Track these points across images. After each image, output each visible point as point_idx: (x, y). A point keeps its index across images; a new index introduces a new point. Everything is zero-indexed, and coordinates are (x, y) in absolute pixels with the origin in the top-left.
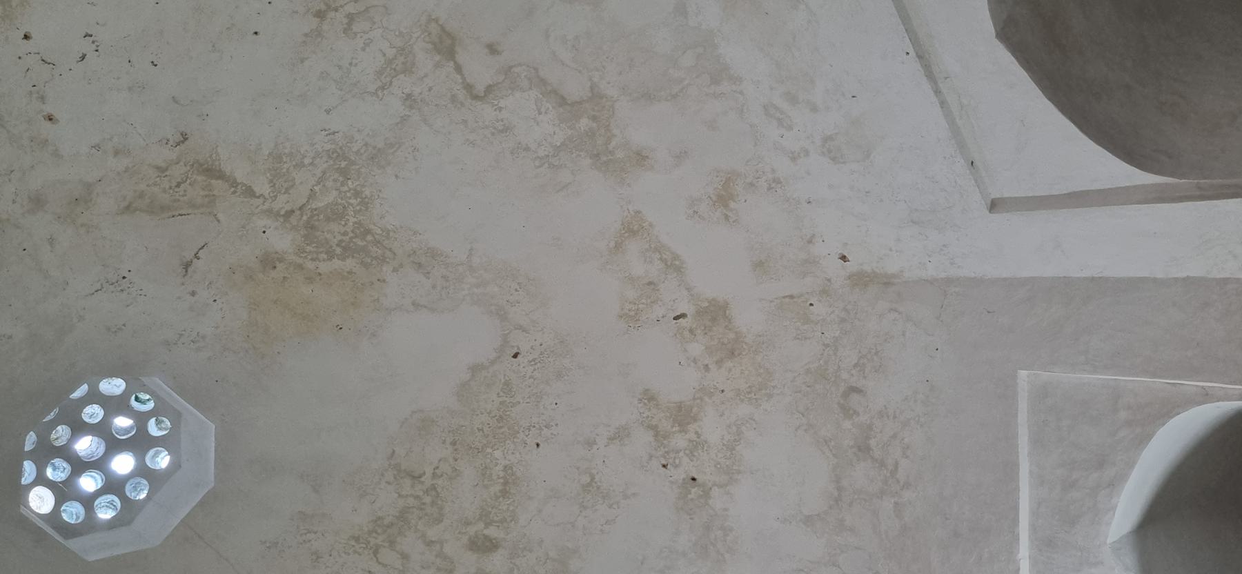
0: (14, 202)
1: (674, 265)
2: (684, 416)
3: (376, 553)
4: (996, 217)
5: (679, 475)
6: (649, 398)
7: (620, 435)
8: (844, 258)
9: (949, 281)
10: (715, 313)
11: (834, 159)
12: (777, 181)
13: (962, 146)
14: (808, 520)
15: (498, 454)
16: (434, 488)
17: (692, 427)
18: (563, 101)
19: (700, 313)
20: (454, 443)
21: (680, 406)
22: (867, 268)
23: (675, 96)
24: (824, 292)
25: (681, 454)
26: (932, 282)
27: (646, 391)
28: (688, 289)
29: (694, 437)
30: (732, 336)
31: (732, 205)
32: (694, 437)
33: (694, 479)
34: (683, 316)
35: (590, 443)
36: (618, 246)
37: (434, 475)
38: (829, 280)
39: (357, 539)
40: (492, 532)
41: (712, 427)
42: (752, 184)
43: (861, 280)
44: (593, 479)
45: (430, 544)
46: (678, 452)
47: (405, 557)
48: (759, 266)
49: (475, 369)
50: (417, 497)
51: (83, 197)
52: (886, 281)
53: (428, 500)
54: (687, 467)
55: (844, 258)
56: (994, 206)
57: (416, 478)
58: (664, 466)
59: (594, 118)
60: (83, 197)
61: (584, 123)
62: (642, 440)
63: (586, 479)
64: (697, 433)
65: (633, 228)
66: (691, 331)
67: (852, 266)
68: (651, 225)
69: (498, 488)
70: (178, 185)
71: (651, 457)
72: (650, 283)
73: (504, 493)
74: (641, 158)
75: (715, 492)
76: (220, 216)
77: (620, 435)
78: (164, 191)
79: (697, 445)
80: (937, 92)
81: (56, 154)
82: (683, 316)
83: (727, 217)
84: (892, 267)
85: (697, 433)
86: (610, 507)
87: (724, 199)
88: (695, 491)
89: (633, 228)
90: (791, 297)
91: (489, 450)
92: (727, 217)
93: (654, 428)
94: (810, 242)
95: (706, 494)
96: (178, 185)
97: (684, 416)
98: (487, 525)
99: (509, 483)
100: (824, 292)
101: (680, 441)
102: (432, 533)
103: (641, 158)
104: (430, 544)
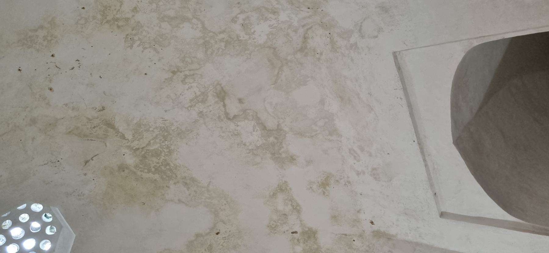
0: (24, 120)
1: (297, 209)
4: (443, 220)
8: (372, 223)
9: (417, 244)
10: (310, 234)
11: (375, 178)
12: (349, 182)
13: (432, 186)
18: (264, 128)
19: (304, 233)
22: (382, 230)
23: (312, 137)
24: (361, 236)
26: (410, 242)
28: (301, 221)
30: (316, 246)
31: (328, 188)
34: (296, 232)
36: (274, 194)
38: (364, 231)
42: (337, 181)
43: (378, 234)
48: (335, 218)
49: (198, 236)
52: (389, 238)
55: (372, 223)
56: (442, 215)
59: (276, 138)
61: (272, 139)
65: (282, 188)
66: (298, 240)
67: (375, 227)
68: (290, 189)
70: (94, 128)
72: (285, 214)
74: (292, 159)
76: (108, 144)
78: (88, 129)
80: (425, 160)
81: (48, 104)
82: (296, 232)
83: (324, 193)
84: (393, 231)
87: (324, 185)
89: (282, 188)
90: (346, 235)
92: (324, 193)
94: (359, 212)
96: (94, 128)
100: (361, 236)
103: (292, 159)
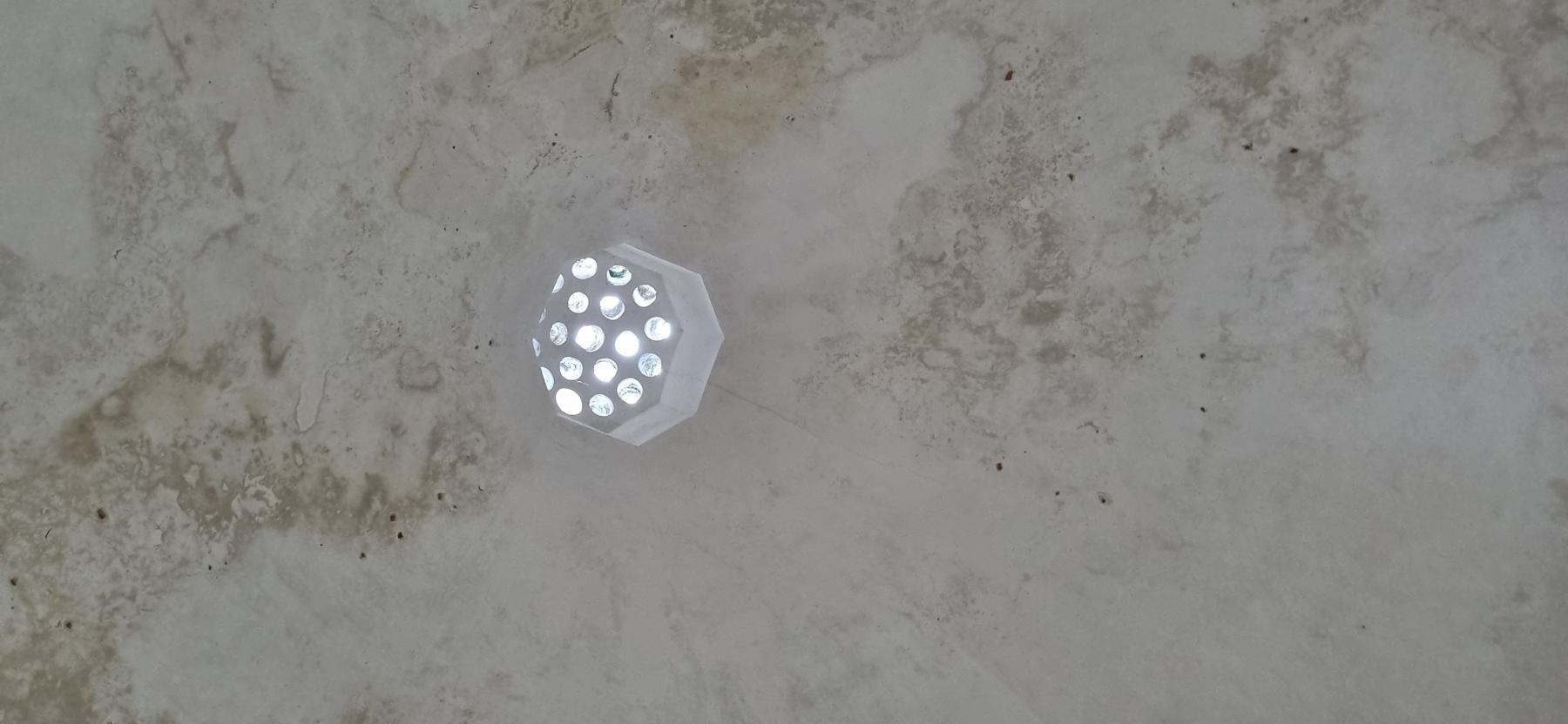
0: (425, 98)
2: (1258, 73)
3: (921, 358)
5: (1271, 152)
6: (1202, 66)
7: (1176, 128)
14: (1480, 151)
15: (1025, 203)
16: (961, 267)
17: (1274, 85)
20: (967, 208)
21: (1248, 63)
25: (1268, 124)
27: (1196, 60)
29: (1278, 95)
32: (1278, 95)
33: (1294, 151)
35: (1138, 152)
37: (958, 254)
39: (895, 349)
40: (1048, 295)
41: (1302, 74)
44: (1154, 192)
45: (977, 330)
46: (1262, 122)
47: (955, 353)
49: (964, 112)
50: (946, 284)
51: (483, 71)
53: (959, 283)
54: (1282, 137)
57: (937, 262)
58: (1247, 148)
60: (483, 71)
62: (1208, 125)
63: (1146, 198)
64: (1285, 91)
69: (1038, 243)
70: (566, 17)
71: (1226, 141)
73: (1048, 247)
75: (1330, 158)
76: (621, 36)
77: (1176, 128)
78: (555, 29)
79: (1287, 106)
81: (440, 29)
85: (1285, 91)
86: (1188, 221)
88: (1299, 167)
91: (1013, 203)
93: (1222, 105)
95: (1317, 162)
96: (566, 17)
97: (1258, 73)
98: (1039, 290)
99: (1049, 231)
101: (1261, 108)
102: (978, 317)
104: (977, 330)
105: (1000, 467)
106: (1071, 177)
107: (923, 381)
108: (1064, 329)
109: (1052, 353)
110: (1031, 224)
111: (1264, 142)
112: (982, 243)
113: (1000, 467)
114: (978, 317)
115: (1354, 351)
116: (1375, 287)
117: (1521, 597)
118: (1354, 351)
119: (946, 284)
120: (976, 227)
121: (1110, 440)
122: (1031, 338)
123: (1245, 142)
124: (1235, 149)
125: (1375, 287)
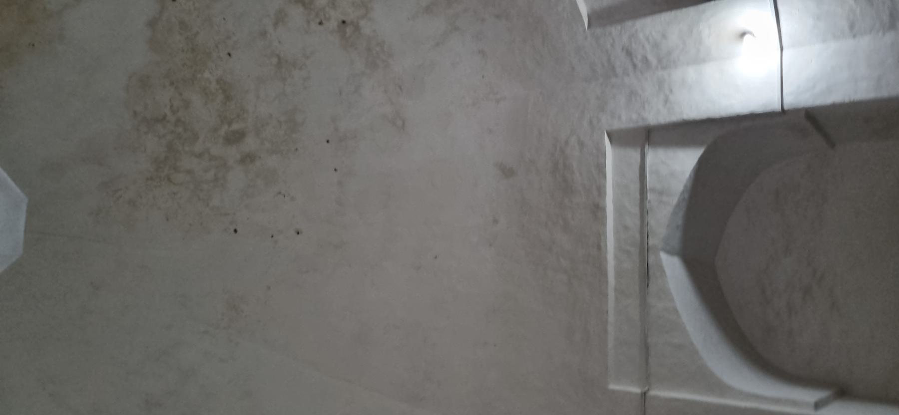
3: (169, 180)
5: (333, 24)
15: (206, 75)
16: (178, 120)
20: (172, 84)
33: (344, 22)
35: (263, 34)
37: (174, 112)
39: (152, 179)
40: (235, 126)
45: (200, 156)
47: (190, 172)
49: (152, 24)
50: (172, 132)
53: (180, 130)
54: (335, 16)
57: (163, 119)
58: (321, 23)
63: (275, 60)
69: (220, 97)
71: (308, 22)
73: (228, 98)
75: (362, 23)
77: (280, 18)
86: (301, 69)
88: (349, 30)
91: (199, 76)
95: (357, 28)
98: (230, 124)
99: (227, 90)
102: (198, 148)
104: (200, 156)
105: (236, 231)
106: (229, 54)
107: (175, 194)
108: (250, 143)
109: (248, 159)
110: (213, 86)
111: (329, 19)
112: (187, 104)
113: (236, 231)
114: (198, 148)
115: (399, 123)
116: (400, 88)
117: (496, 221)
118: (399, 123)
119: (172, 132)
120: (181, 94)
121: (293, 199)
122: (232, 153)
123: (318, 20)
124: (314, 26)
125: (400, 88)
